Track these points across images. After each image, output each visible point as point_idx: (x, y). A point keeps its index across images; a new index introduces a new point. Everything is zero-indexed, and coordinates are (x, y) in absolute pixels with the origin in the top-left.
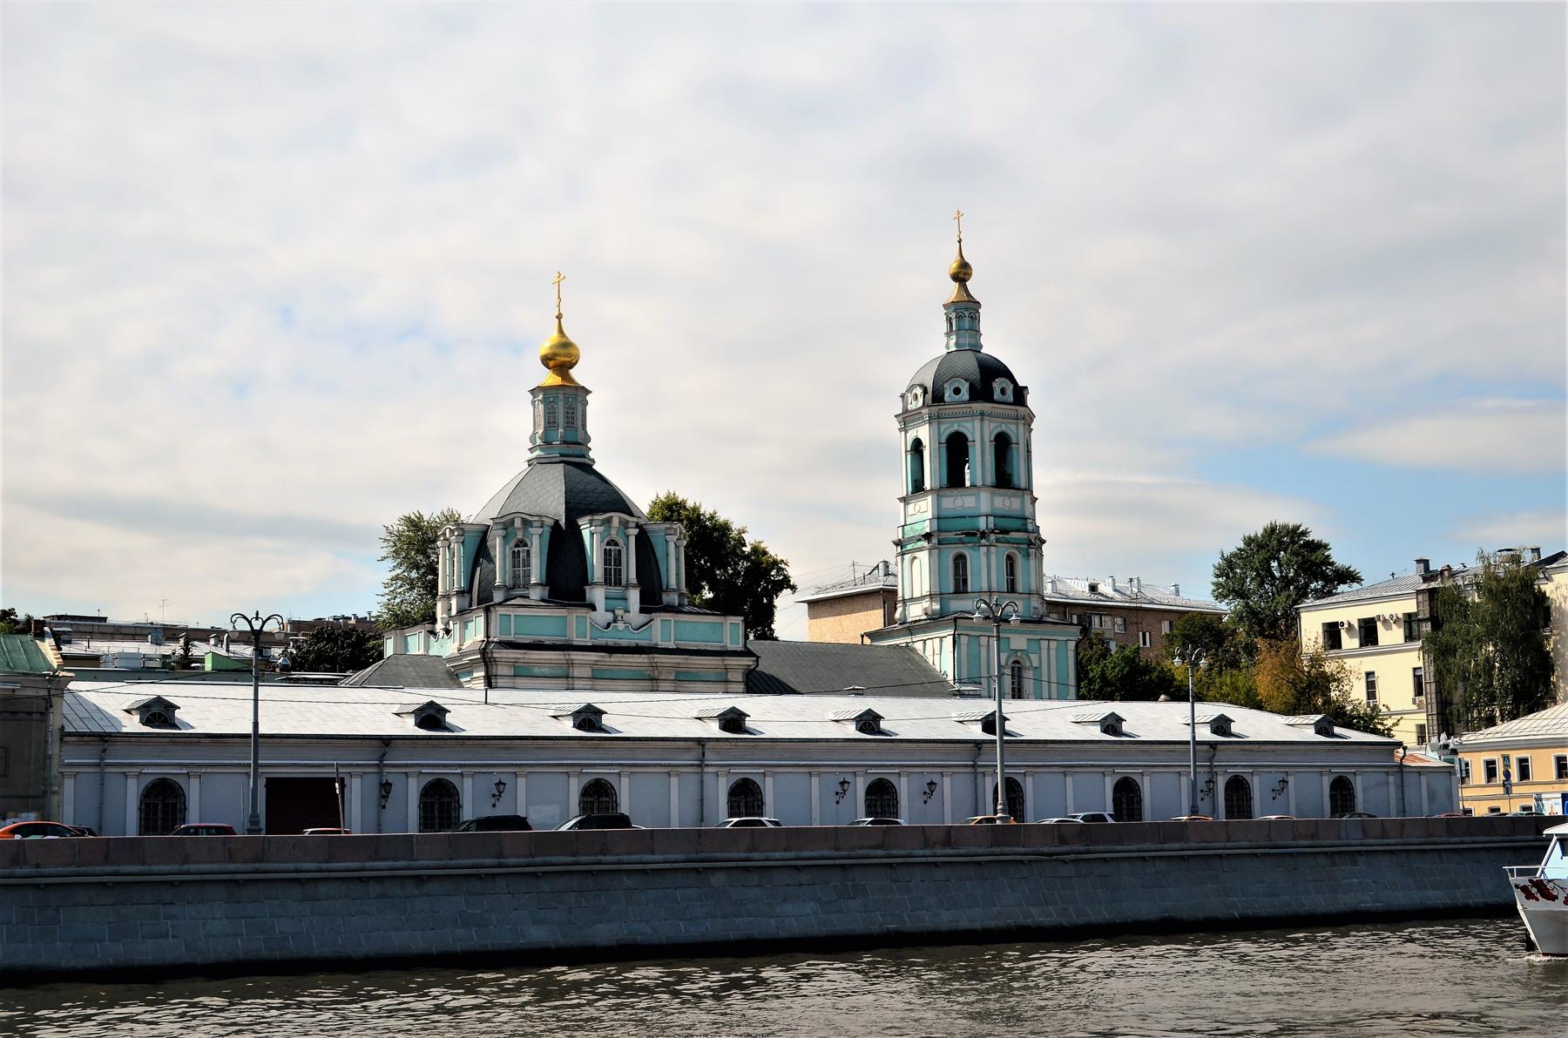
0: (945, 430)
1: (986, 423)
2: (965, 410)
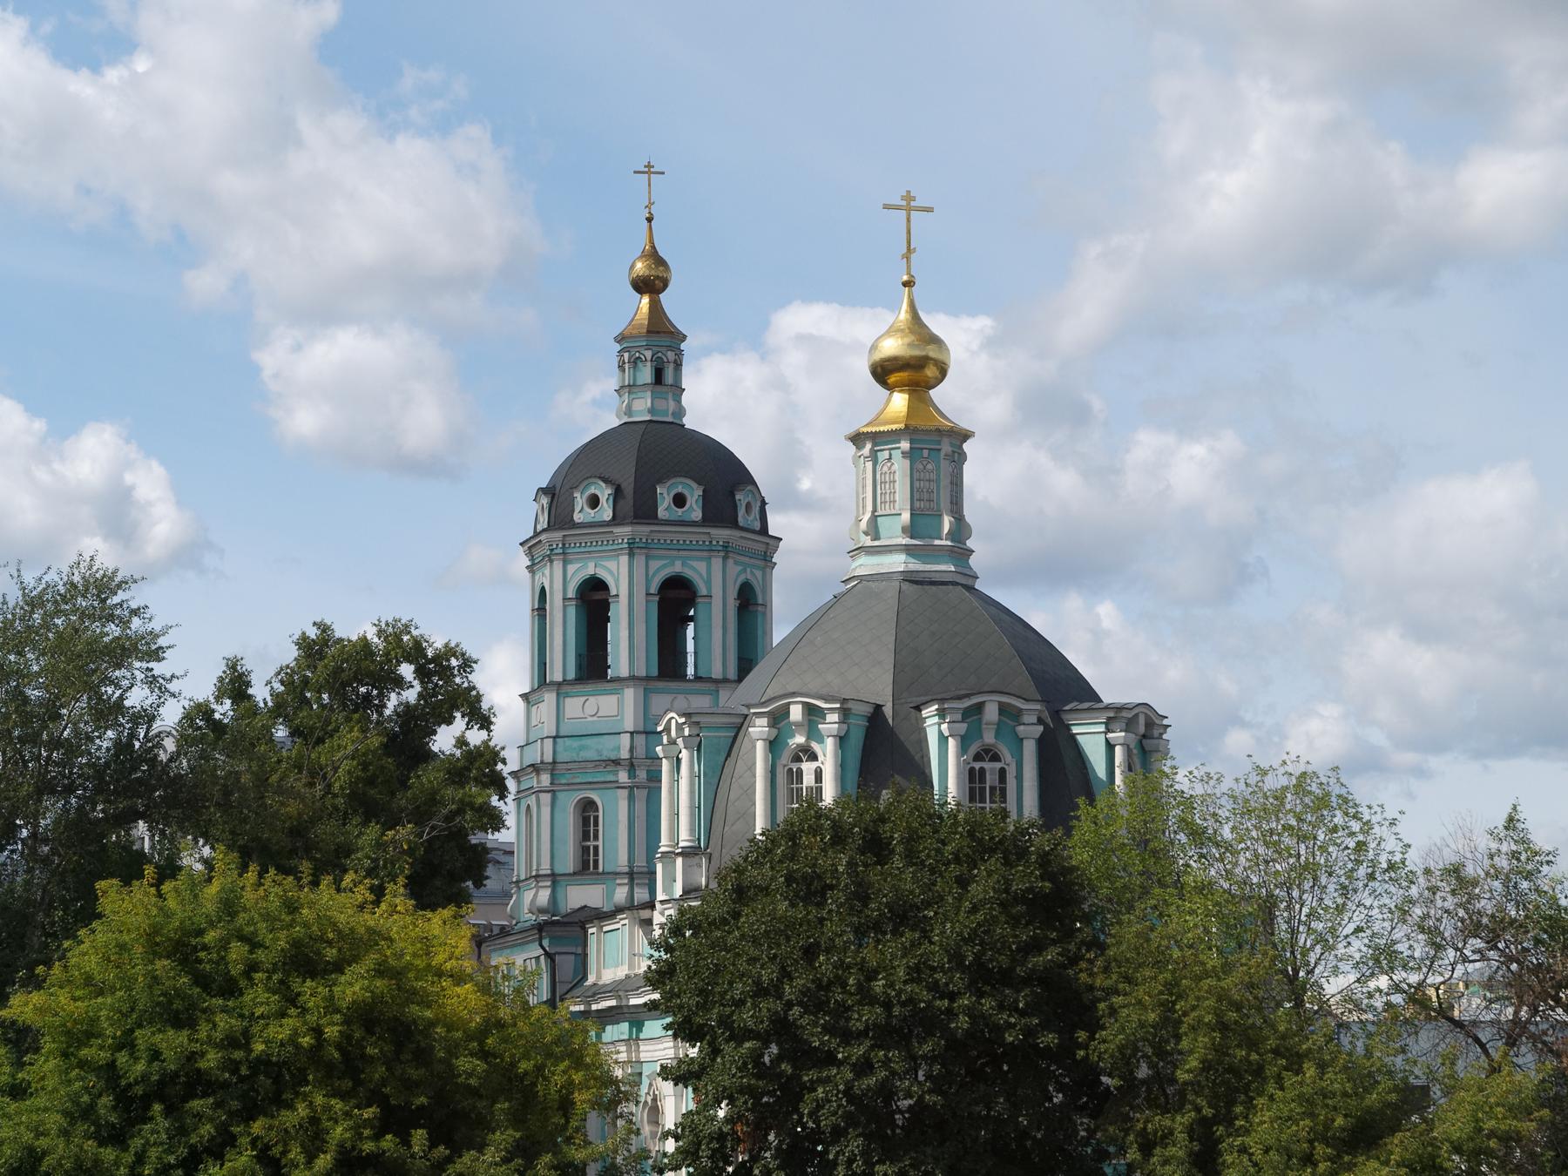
0: (658, 570)
1: (730, 562)
2: (694, 538)
